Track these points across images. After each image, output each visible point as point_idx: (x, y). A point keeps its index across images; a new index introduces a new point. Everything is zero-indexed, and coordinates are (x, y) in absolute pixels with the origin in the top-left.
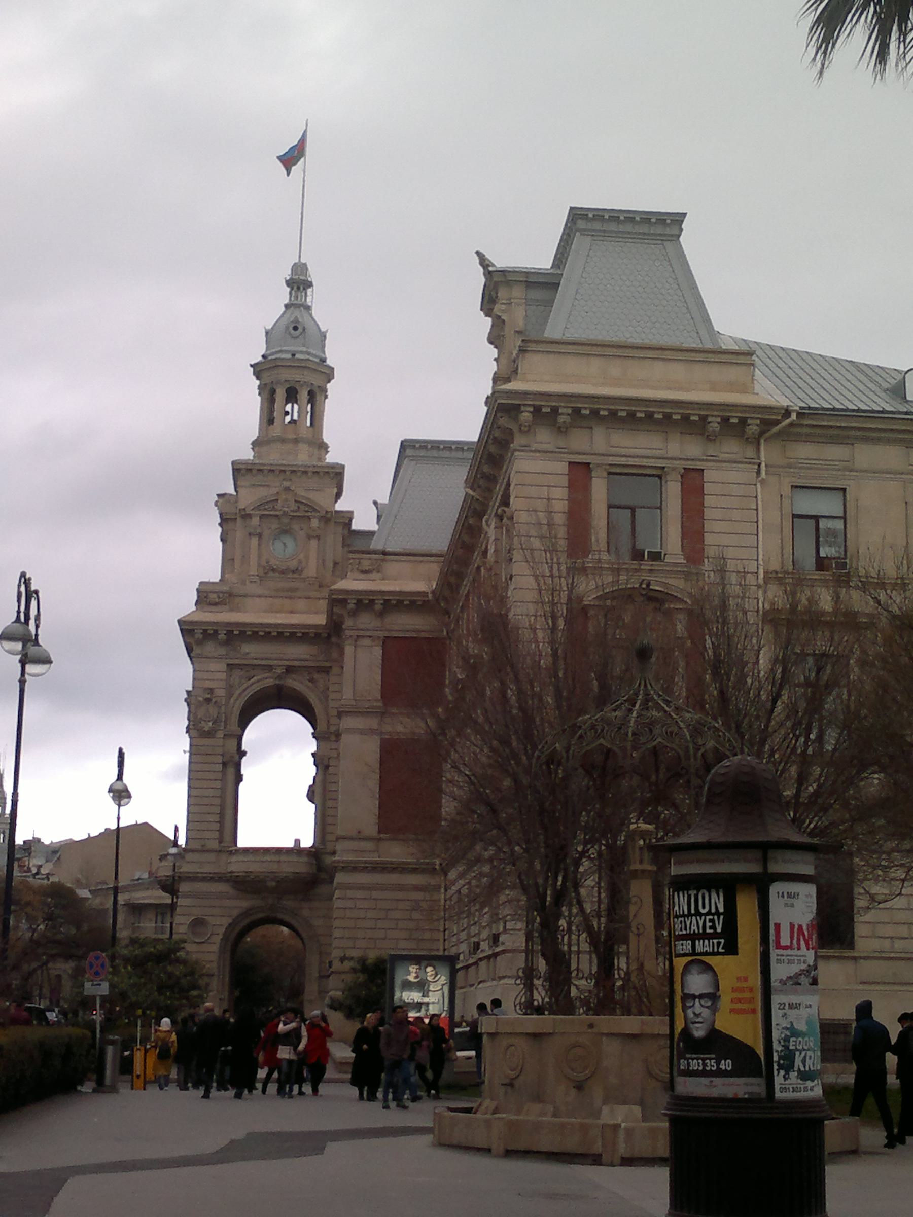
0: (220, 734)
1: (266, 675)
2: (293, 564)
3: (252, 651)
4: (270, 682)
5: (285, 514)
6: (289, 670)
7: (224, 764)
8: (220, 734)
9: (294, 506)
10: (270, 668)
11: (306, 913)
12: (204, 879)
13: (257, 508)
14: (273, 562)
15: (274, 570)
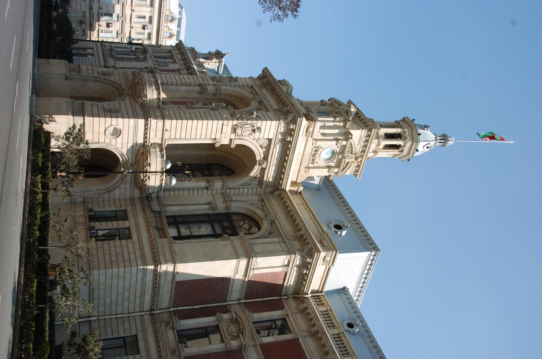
0: (233, 136)
1: (262, 156)
2: (317, 160)
3: (276, 151)
4: (258, 158)
5: (344, 157)
6: (263, 170)
7: (215, 139)
8: (233, 136)
9: (347, 160)
10: (266, 158)
11: (123, 186)
12: (145, 133)
13: (351, 144)
14: (321, 150)
15: (316, 151)
